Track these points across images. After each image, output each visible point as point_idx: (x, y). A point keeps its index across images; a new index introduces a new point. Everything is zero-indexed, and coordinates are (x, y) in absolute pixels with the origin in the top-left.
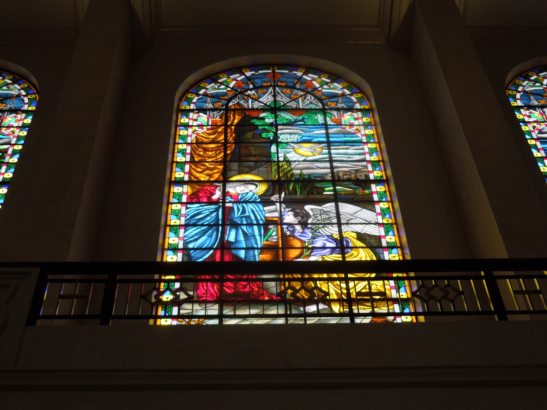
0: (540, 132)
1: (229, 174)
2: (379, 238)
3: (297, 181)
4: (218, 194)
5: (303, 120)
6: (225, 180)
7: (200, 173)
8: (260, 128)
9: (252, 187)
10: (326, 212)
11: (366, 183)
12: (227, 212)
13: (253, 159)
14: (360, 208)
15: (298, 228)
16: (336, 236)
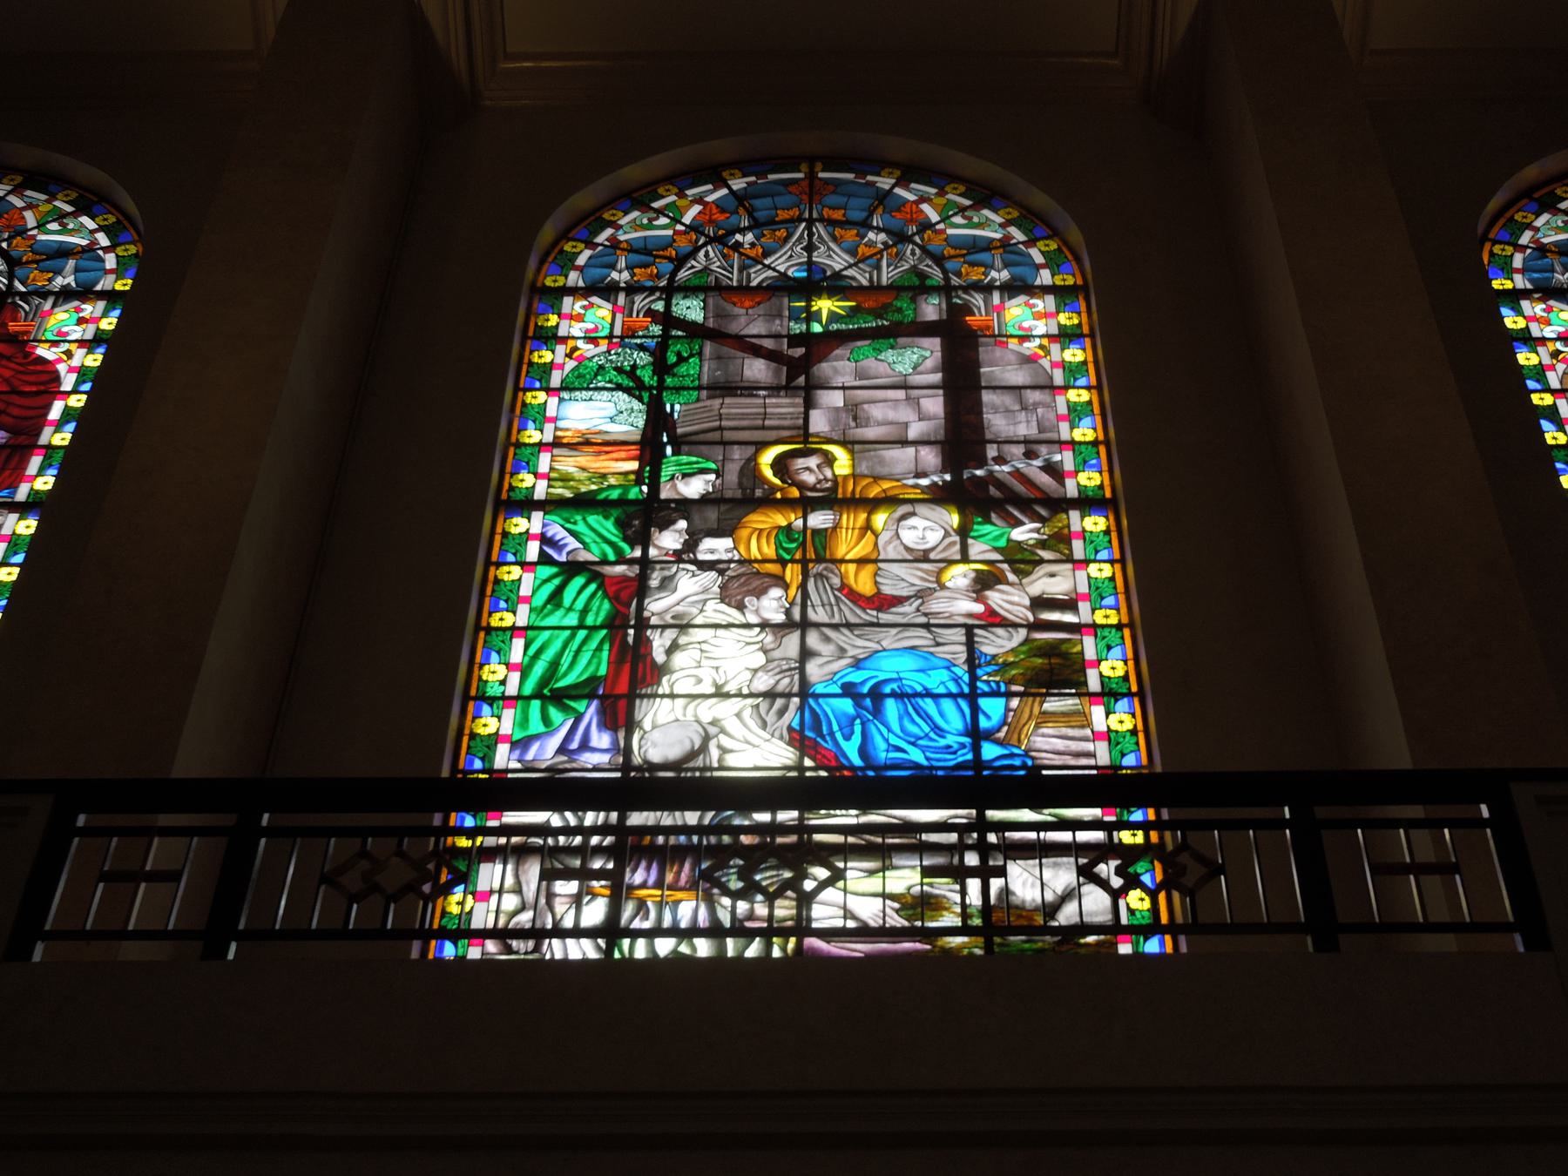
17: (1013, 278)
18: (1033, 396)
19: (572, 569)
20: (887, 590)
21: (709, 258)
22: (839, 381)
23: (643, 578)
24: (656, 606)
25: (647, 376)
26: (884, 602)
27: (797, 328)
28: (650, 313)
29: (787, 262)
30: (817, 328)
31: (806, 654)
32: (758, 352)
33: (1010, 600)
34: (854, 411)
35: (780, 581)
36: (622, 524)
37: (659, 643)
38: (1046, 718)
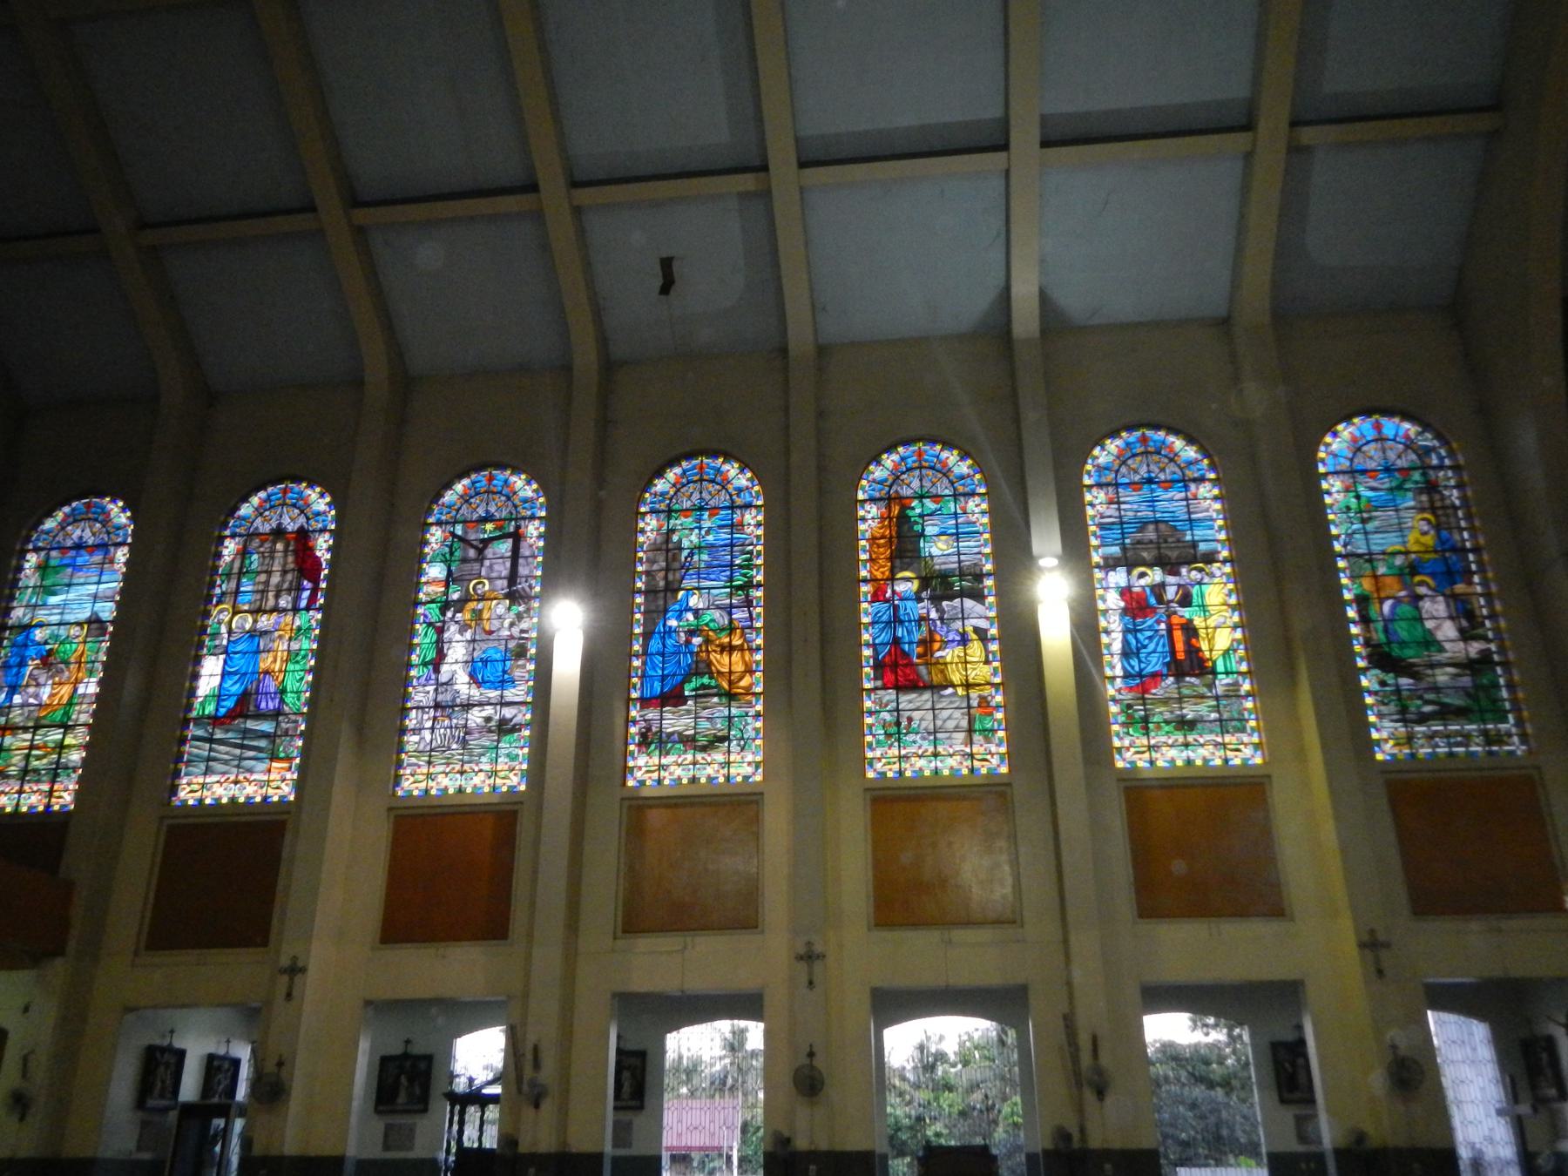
0: (1102, 517)
1: (896, 570)
2: (986, 631)
3: (937, 577)
4: (889, 591)
5: (940, 510)
6: (892, 579)
7: (877, 570)
8: (913, 519)
9: (909, 584)
10: (955, 608)
11: (979, 577)
12: (896, 608)
13: (910, 554)
14: (975, 603)
15: (938, 622)
16: (961, 630)
17: (533, 514)
18: (530, 560)
19: (430, 624)
20: (493, 629)
21: (465, 509)
22: (490, 556)
23: (443, 627)
24: (446, 635)
25: (448, 556)
26: (491, 633)
27: (482, 536)
28: (450, 532)
29: (481, 512)
30: (486, 536)
31: (474, 649)
32: (473, 546)
33: (515, 631)
34: (491, 567)
35: (470, 627)
36: (440, 609)
37: (446, 646)
38: (518, 666)
